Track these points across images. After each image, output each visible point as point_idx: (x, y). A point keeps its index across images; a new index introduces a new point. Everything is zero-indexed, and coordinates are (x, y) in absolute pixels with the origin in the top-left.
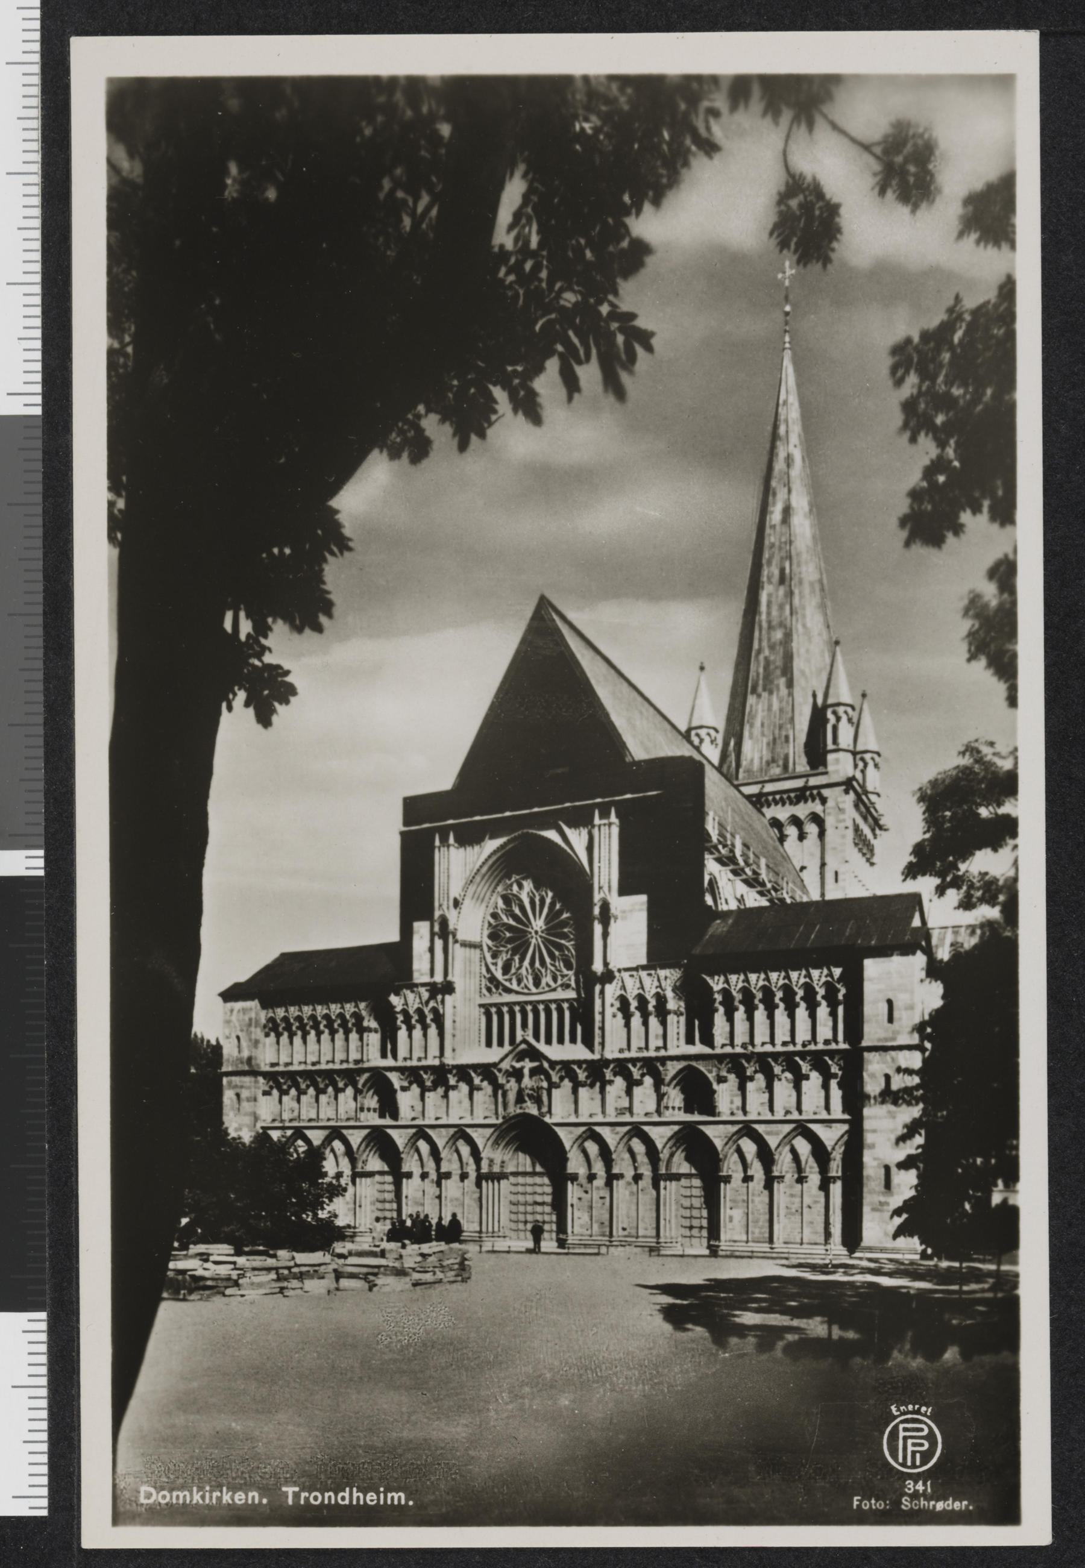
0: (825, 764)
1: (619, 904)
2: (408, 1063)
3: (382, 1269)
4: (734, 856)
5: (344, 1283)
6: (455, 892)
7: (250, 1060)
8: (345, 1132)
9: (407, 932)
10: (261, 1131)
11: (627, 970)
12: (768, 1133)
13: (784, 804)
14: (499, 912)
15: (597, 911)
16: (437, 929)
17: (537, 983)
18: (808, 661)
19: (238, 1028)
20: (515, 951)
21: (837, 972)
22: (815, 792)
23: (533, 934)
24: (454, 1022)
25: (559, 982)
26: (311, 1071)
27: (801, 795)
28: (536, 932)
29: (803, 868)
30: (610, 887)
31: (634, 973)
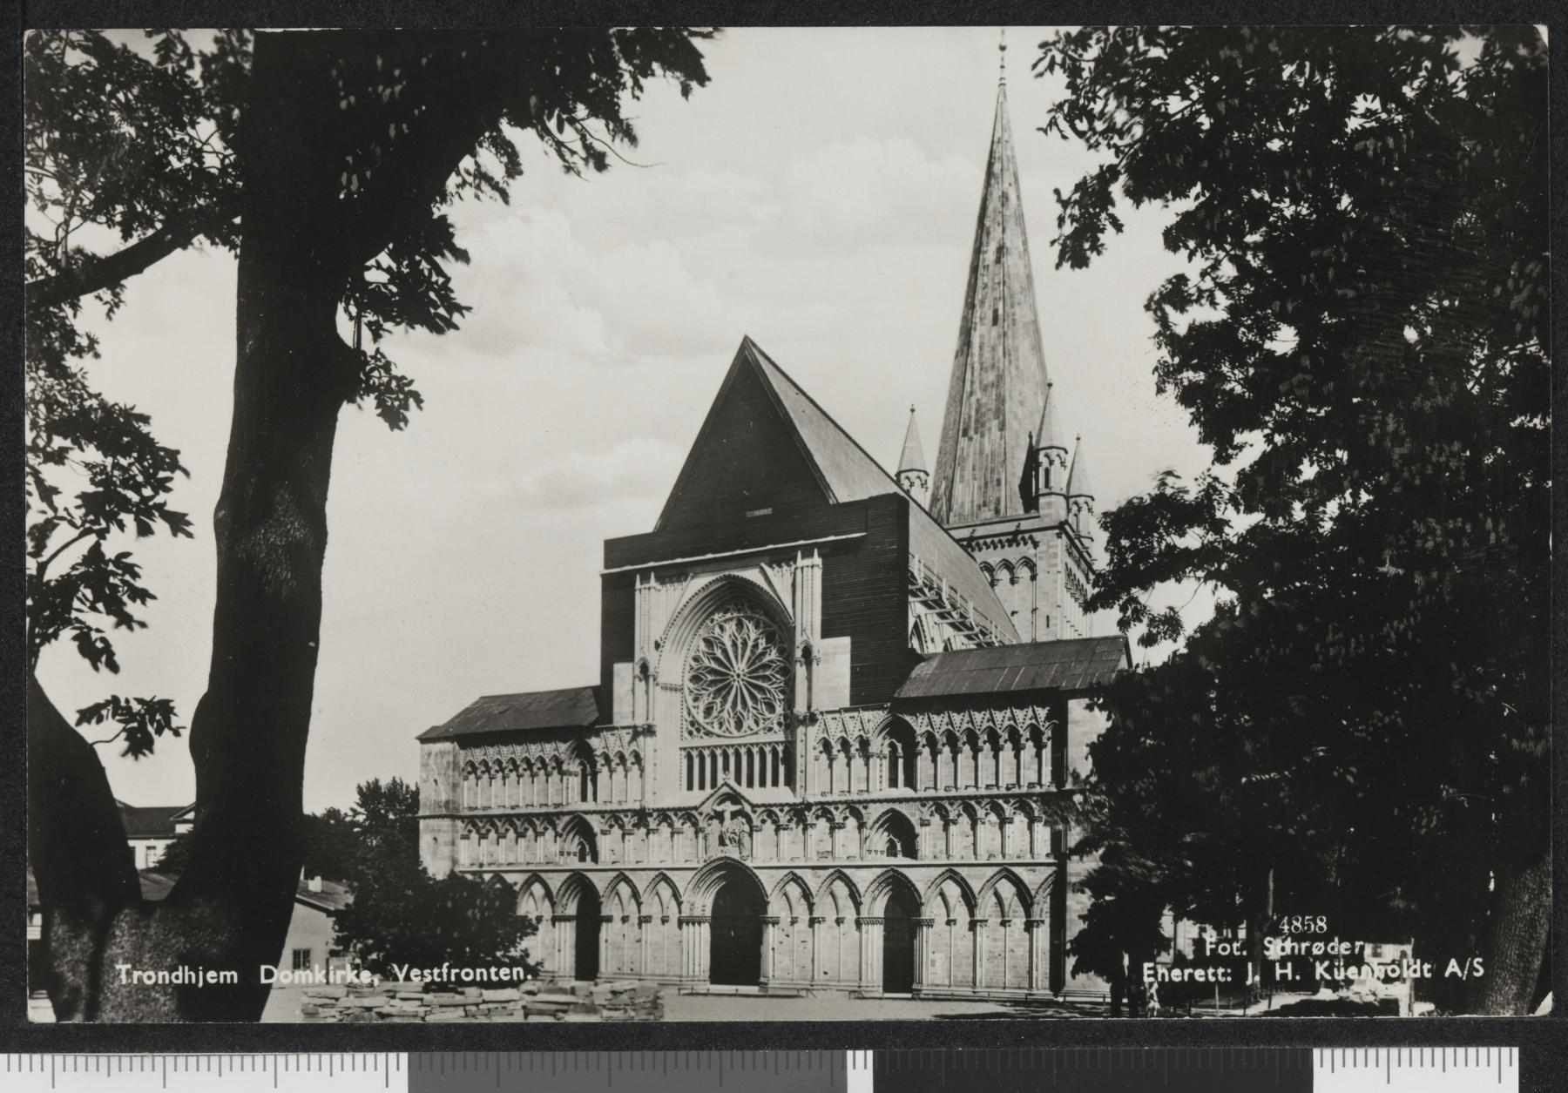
0: (1037, 509)
1: (821, 646)
2: (609, 807)
3: (572, 1006)
6: (656, 634)
7: (447, 803)
11: (828, 712)
12: (974, 877)
14: (702, 656)
15: (798, 653)
16: (637, 671)
17: (739, 724)
19: (436, 772)
23: (735, 677)
25: (761, 725)
27: (1014, 538)
28: (738, 676)
29: (1014, 613)
31: (837, 715)
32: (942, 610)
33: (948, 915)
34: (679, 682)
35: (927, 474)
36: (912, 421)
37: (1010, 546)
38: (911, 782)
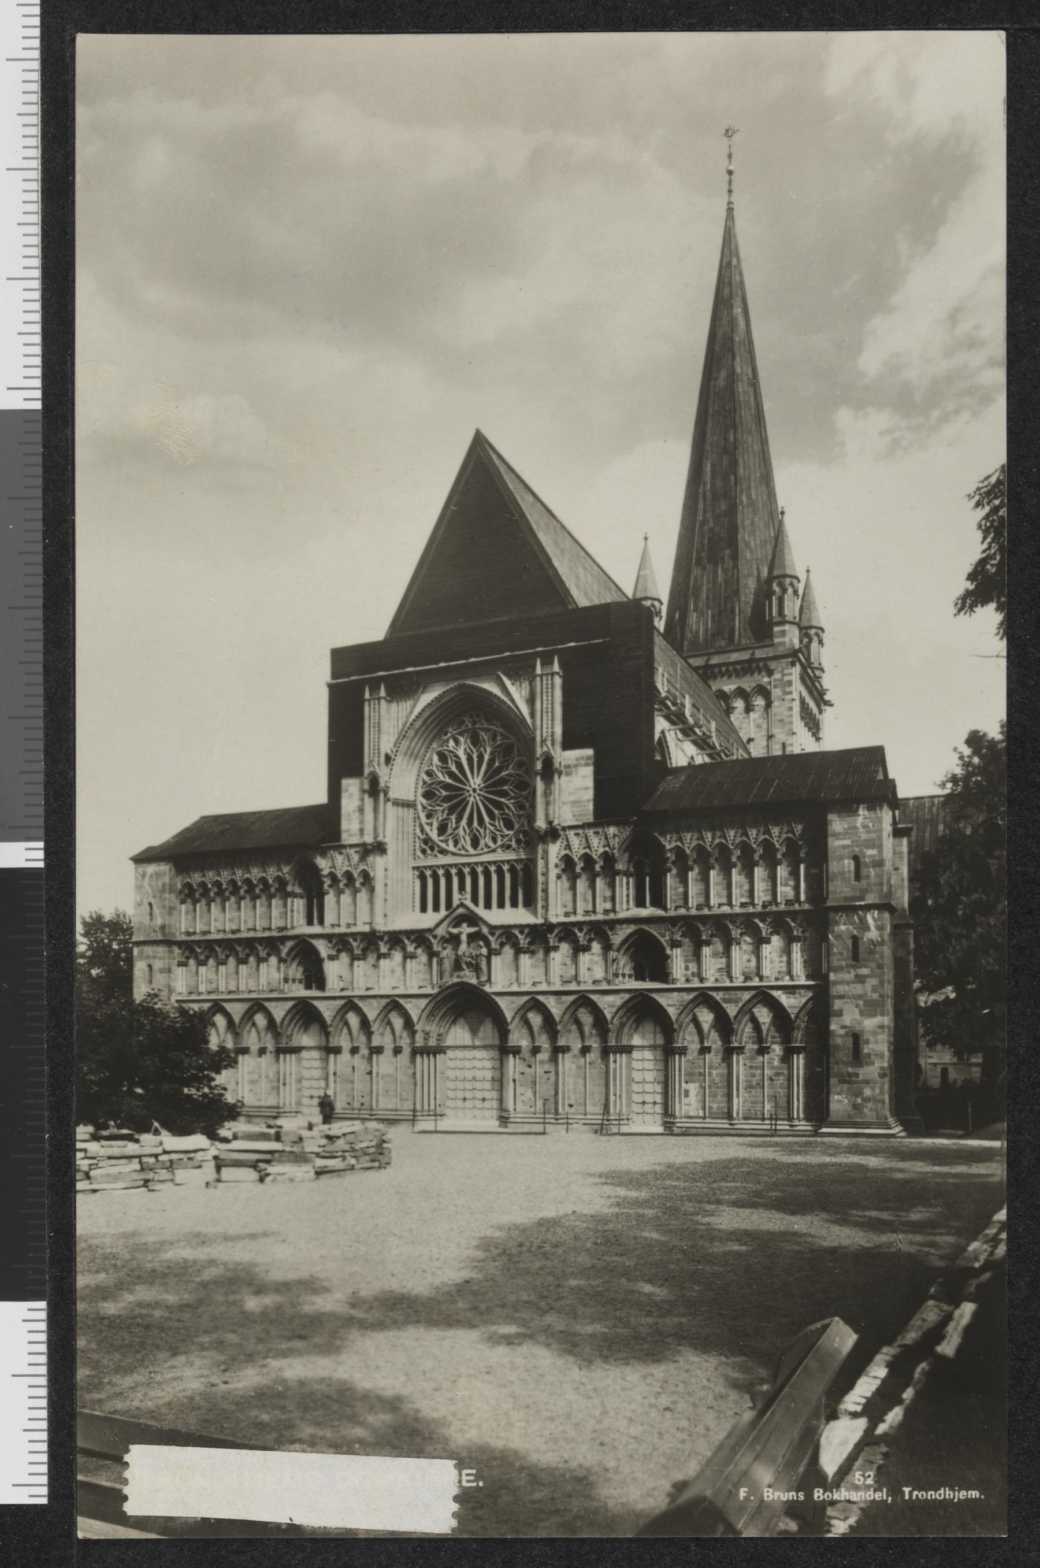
0: (771, 636)
2: (337, 930)
3: (277, 1155)
4: (683, 714)
5: (227, 1173)
6: (387, 745)
7: (163, 927)
8: (267, 1004)
9: (335, 791)
10: (176, 1005)
11: (571, 827)
13: (729, 677)
14: (435, 769)
15: (539, 766)
16: (366, 787)
17: (475, 843)
18: (753, 532)
19: (151, 894)
20: (451, 810)
21: (799, 828)
22: (761, 664)
24: (386, 885)
25: (499, 843)
26: (229, 940)
27: (748, 668)
28: (474, 790)
29: (750, 740)
30: (553, 740)
31: (581, 831)
33: (702, 1042)
34: (412, 798)
35: (661, 603)
37: (745, 674)
38: (659, 901)
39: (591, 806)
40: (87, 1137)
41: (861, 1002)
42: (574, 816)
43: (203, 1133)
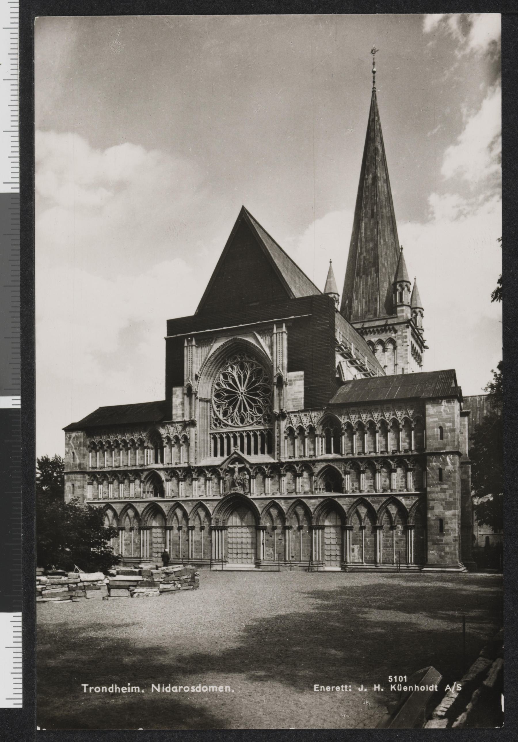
0: (396, 312)
1: (288, 376)
2: (170, 466)
4: (350, 353)
5: (113, 592)
7: (80, 465)
8: (134, 504)
9: (169, 394)
10: (87, 505)
11: (292, 412)
14: (221, 382)
15: (275, 380)
16: (185, 392)
17: (242, 421)
18: (386, 259)
20: (230, 404)
21: (411, 412)
22: (391, 327)
23: (240, 394)
24: (196, 442)
25: (255, 420)
26: (115, 471)
27: (384, 329)
28: (242, 393)
29: (385, 366)
30: (282, 367)
31: (297, 414)
32: (352, 359)
33: (361, 524)
34: (210, 398)
35: (339, 296)
36: (331, 266)
37: (383, 332)
38: (338, 450)
39: (302, 401)
40: (40, 573)
41: (444, 503)
42: (294, 406)
43: (101, 572)
